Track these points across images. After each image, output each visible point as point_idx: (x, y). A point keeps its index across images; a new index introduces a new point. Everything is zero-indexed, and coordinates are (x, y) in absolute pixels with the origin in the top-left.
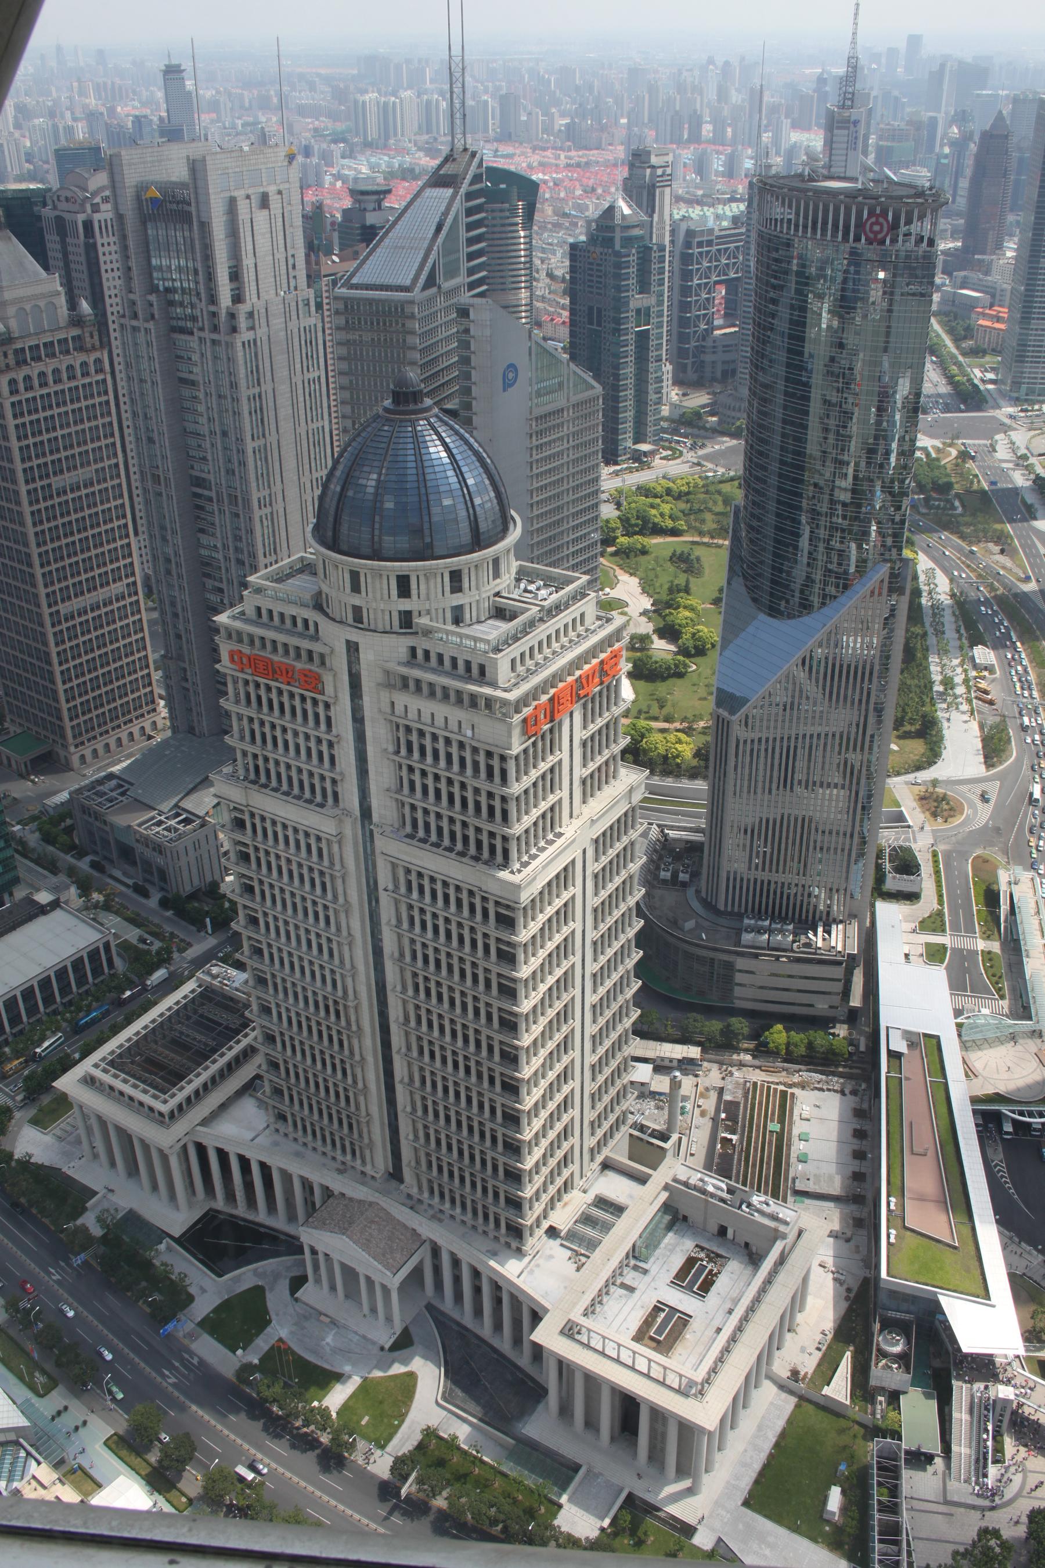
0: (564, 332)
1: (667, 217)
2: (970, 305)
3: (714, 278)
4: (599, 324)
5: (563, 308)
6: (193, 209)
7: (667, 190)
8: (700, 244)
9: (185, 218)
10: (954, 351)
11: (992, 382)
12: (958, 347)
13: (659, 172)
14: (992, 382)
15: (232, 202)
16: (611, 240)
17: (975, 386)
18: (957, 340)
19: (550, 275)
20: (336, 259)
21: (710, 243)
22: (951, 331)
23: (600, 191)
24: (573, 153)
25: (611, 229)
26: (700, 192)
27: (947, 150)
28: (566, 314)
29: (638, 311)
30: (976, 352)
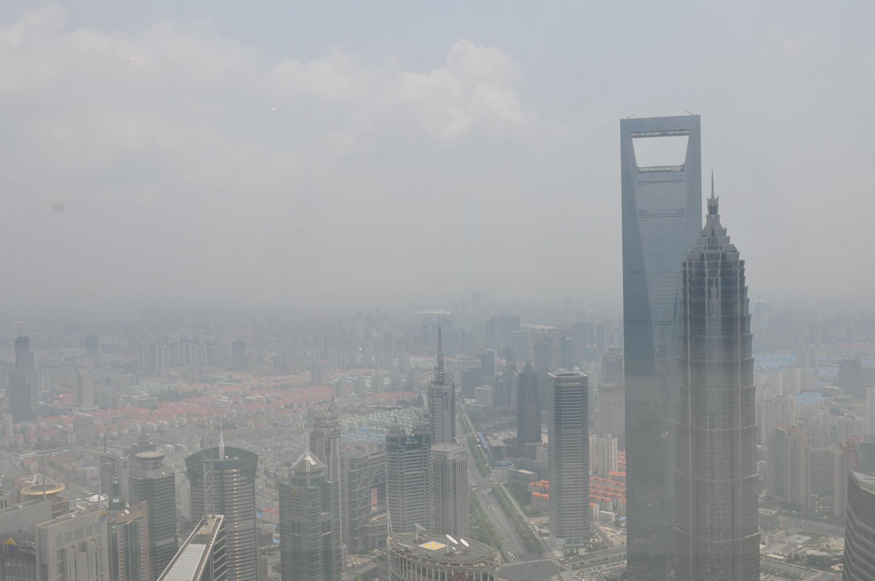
0: (276, 518)
1: (338, 455)
2: (528, 479)
3: (369, 485)
4: (299, 533)
5: (275, 500)
6: (37, 554)
7: (338, 439)
8: (359, 466)
9: (32, 559)
10: (521, 513)
11: (547, 535)
12: (523, 510)
13: (332, 429)
14: (547, 535)
15: (62, 554)
16: (305, 481)
17: (536, 540)
18: (522, 505)
19: (267, 473)
20: (127, 512)
21: (365, 465)
22: (517, 498)
23: (296, 406)
24: (278, 378)
25: (305, 474)
26: (357, 405)
27: (501, 374)
28: (277, 504)
29: (323, 523)
30: (535, 514)
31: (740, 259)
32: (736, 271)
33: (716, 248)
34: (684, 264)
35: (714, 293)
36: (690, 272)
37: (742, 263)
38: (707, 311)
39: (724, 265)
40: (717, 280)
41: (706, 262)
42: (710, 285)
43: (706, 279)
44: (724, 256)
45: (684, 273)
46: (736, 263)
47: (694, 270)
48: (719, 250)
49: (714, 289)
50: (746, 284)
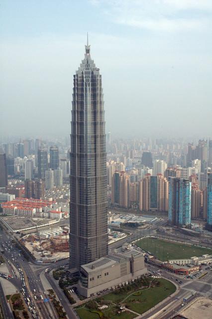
31: (100, 74)
32: (98, 79)
33: (89, 69)
34: (74, 76)
35: (88, 90)
36: (77, 80)
37: (100, 76)
38: (85, 98)
39: (92, 77)
40: (89, 84)
41: (84, 75)
42: (86, 86)
43: (84, 83)
44: (92, 73)
45: (74, 80)
46: (98, 76)
47: (79, 79)
48: (90, 70)
49: (88, 87)
50: (102, 87)
